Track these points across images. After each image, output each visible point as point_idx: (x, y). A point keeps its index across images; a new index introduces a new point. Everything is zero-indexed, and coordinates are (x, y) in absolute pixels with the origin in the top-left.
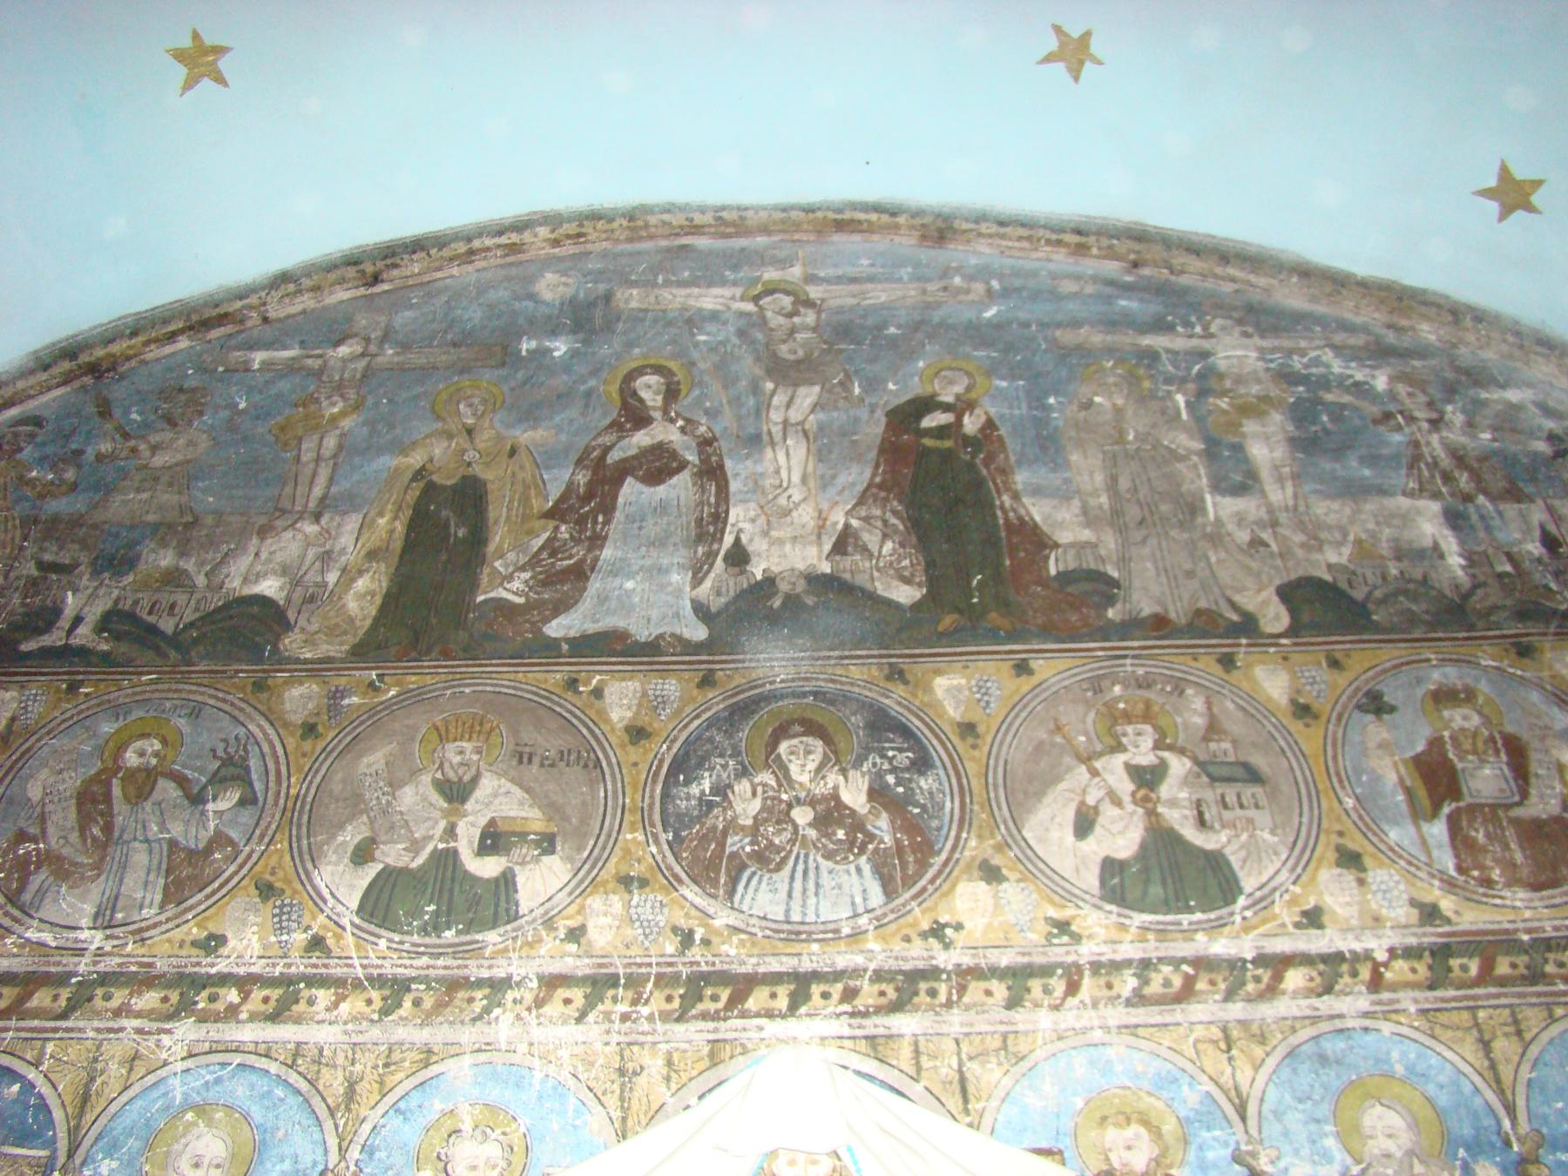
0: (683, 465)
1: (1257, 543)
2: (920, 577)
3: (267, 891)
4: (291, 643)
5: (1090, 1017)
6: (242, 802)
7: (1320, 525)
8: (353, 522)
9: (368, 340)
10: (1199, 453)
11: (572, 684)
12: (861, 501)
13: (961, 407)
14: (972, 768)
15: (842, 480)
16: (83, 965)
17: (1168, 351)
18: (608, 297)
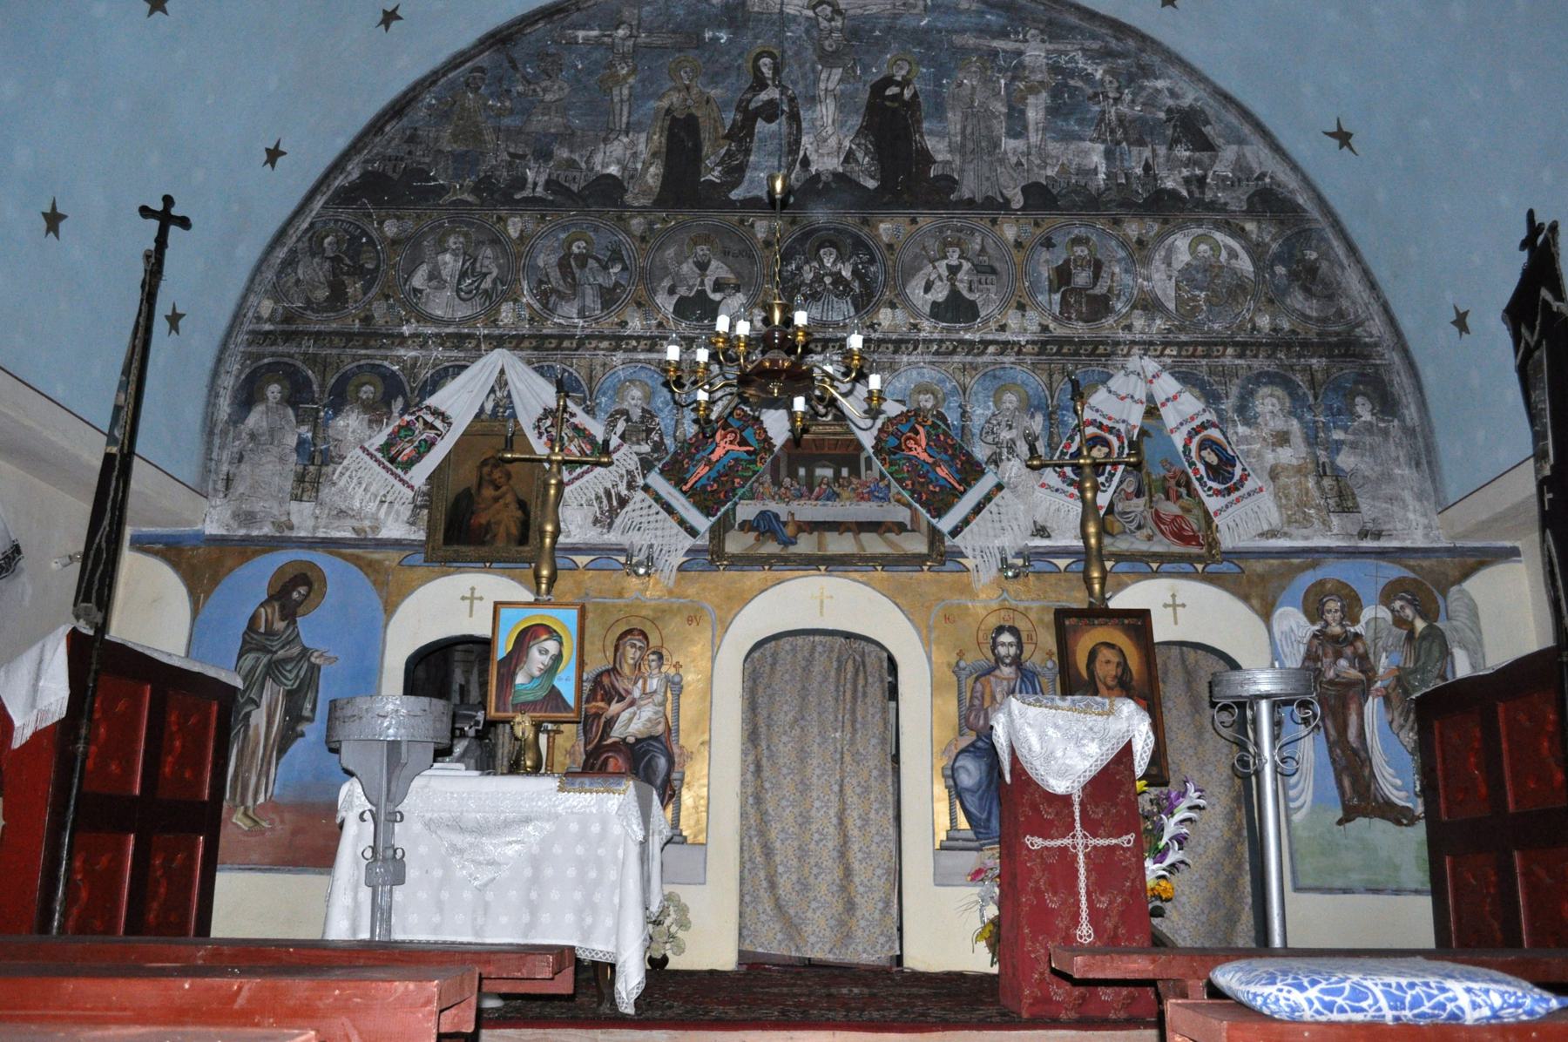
0: (783, 111)
1: (1019, 164)
2: (878, 176)
3: (639, 305)
4: (628, 198)
5: (919, 358)
6: (625, 269)
7: (1048, 156)
10: (1004, 114)
11: (742, 221)
12: (856, 136)
14: (890, 263)
15: (849, 123)
16: (578, 332)
17: (1005, 51)
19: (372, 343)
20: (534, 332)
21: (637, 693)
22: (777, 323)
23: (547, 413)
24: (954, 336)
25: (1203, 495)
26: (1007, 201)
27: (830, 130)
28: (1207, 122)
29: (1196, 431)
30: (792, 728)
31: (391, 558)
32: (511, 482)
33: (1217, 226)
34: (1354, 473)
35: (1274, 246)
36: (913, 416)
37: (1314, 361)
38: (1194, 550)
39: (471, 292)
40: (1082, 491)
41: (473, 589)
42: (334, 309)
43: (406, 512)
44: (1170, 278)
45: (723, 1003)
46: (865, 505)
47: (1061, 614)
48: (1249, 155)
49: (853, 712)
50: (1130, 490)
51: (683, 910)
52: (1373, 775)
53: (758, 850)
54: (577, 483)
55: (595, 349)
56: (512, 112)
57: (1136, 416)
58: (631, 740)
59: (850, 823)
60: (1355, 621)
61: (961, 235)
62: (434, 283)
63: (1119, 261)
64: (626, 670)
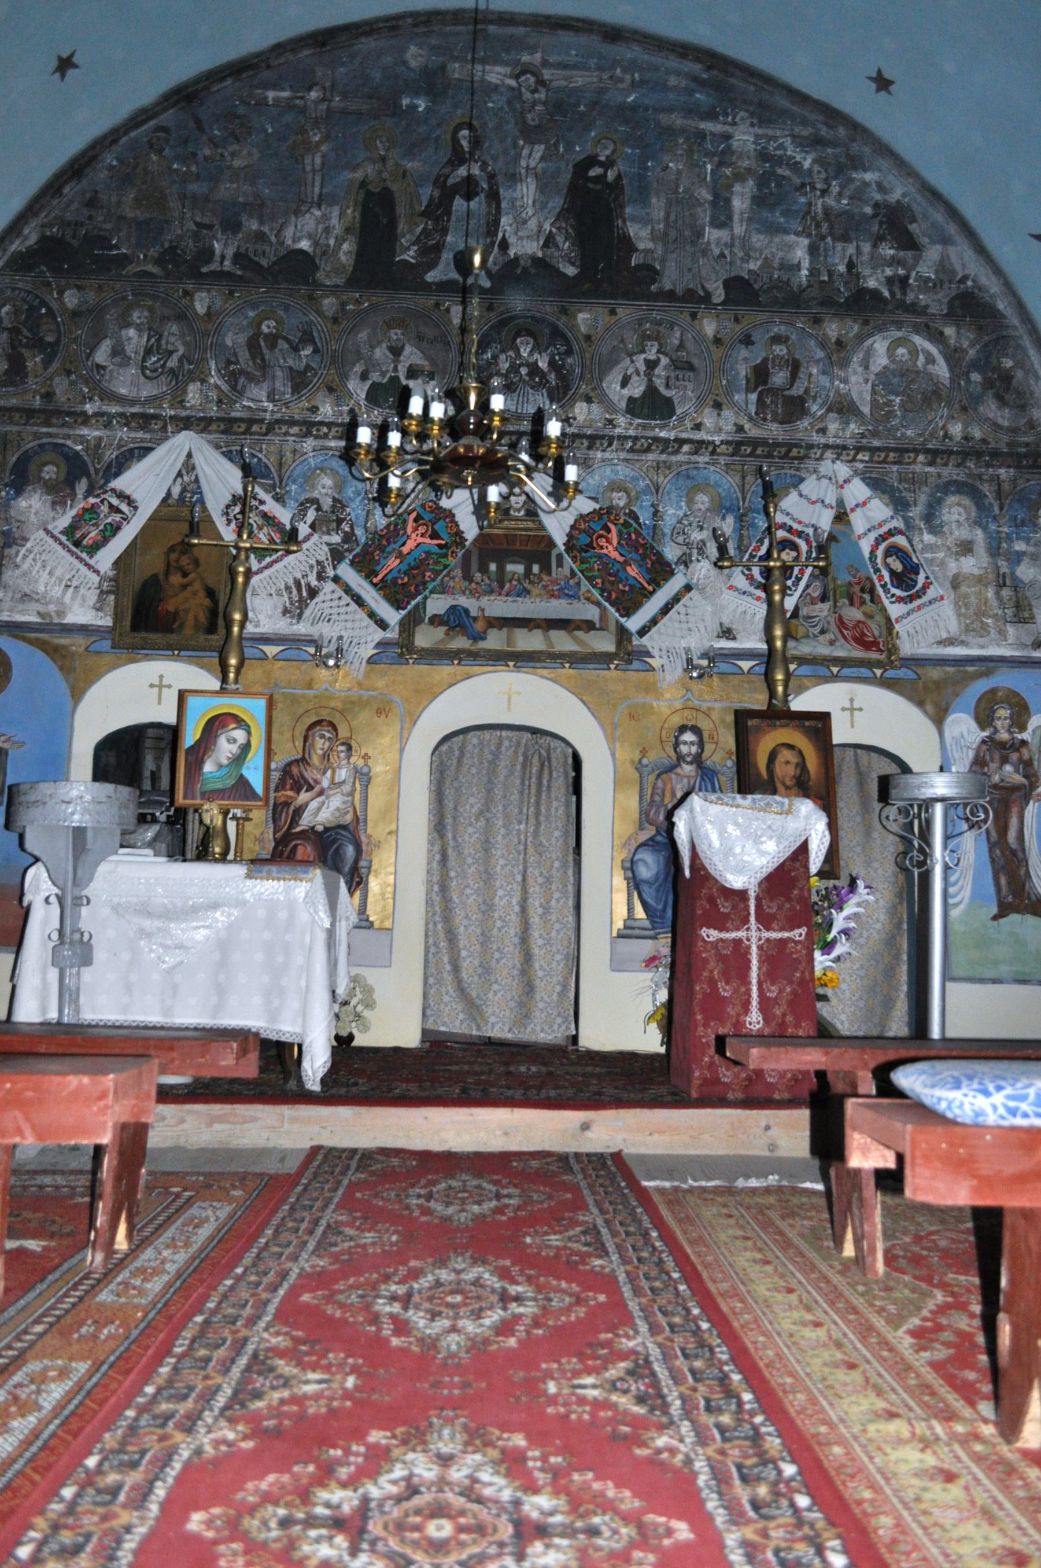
1: (722, 256)
3: (331, 390)
4: (320, 276)
5: (614, 455)
6: (316, 351)
7: (751, 248)
8: (336, 211)
9: (324, 88)
11: (437, 305)
12: (558, 218)
13: (609, 164)
17: (712, 134)
18: (443, 68)
19: (54, 421)
20: (222, 414)
21: (325, 783)
22: (472, 407)
23: (235, 499)
24: (650, 434)
25: (886, 602)
26: (708, 295)
27: (530, 211)
28: (914, 220)
29: (883, 538)
30: (477, 820)
31: (77, 643)
32: (200, 570)
33: (918, 333)
34: (1032, 584)
35: (972, 352)
36: (604, 515)
37: (1002, 471)
38: (874, 655)
39: (155, 370)
40: (769, 593)
41: (161, 677)
42: (13, 384)
43: (92, 597)
44: (867, 381)
45: (407, 1081)
46: (555, 602)
47: (741, 717)
48: (954, 258)
49: (538, 804)
50: (816, 594)
51: (368, 990)
52: (1028, 873)
53: (442, 936)
54: (267, 573)
55: (286, 434)
56: (198, 177)
57: (825, 521)
58: (320, 828)
59: (531, 912)
60: (1023, 728)
61: (661, 329)
62: (117, 359)
63: (817, 361)
64: (315, 760)
